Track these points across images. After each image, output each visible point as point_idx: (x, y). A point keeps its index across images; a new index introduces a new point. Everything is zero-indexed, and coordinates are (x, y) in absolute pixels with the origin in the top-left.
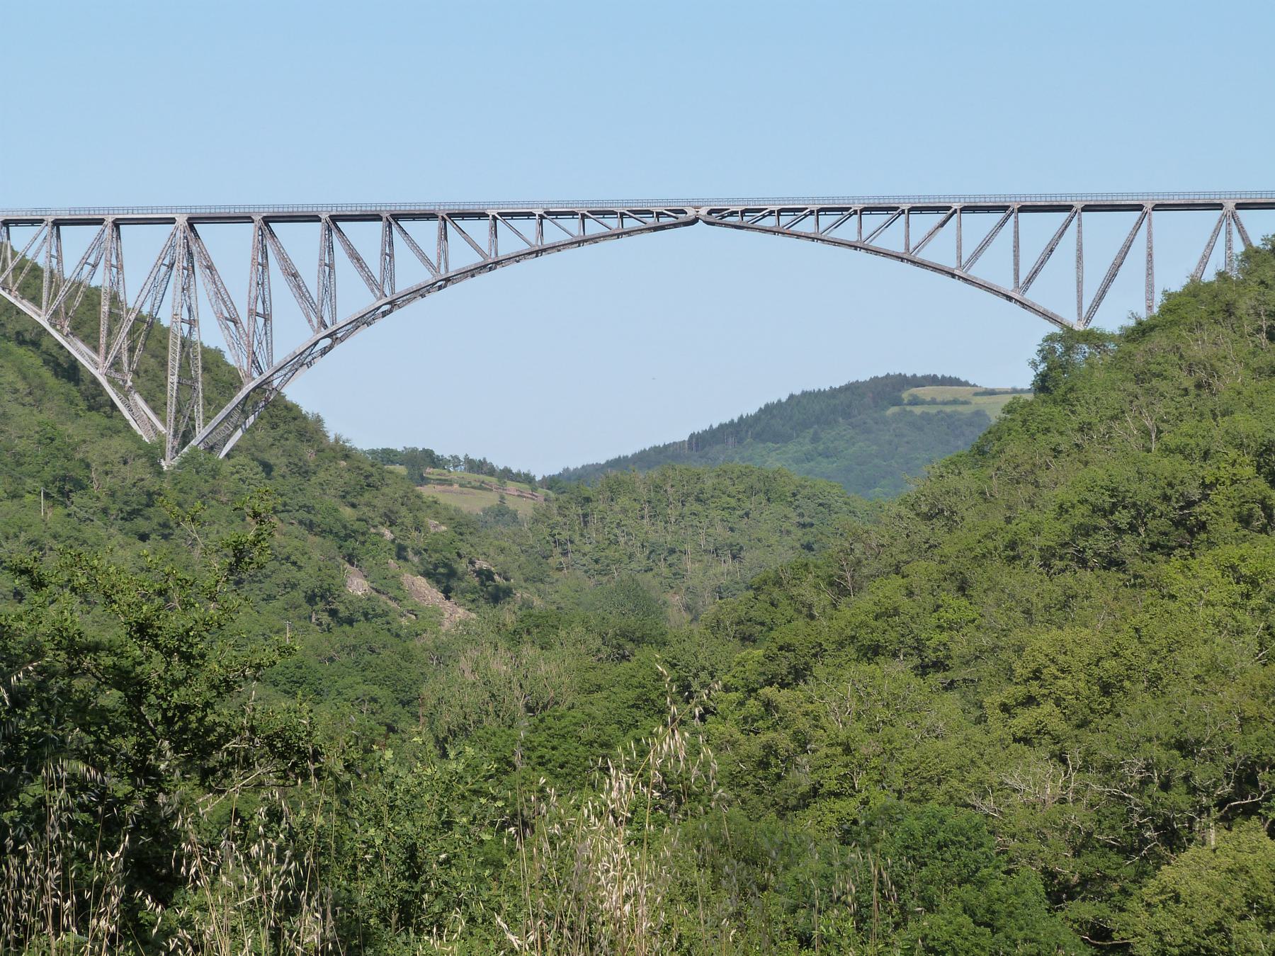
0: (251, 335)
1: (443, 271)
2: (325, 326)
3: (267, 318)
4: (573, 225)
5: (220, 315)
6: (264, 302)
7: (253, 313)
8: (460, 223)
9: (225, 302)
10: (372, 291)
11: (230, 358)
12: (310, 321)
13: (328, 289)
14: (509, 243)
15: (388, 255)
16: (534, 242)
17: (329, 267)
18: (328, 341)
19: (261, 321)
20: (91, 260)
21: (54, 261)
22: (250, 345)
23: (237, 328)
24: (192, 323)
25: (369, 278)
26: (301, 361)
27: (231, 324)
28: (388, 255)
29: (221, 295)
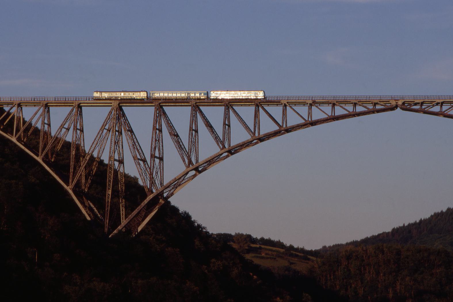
1: (257, 134)
2: (193, 164)
12: (184, 161)
13: (194, 142)
15: (227, 125)
17: (194, 131)
18: (193, 172)
25: (216, 138)
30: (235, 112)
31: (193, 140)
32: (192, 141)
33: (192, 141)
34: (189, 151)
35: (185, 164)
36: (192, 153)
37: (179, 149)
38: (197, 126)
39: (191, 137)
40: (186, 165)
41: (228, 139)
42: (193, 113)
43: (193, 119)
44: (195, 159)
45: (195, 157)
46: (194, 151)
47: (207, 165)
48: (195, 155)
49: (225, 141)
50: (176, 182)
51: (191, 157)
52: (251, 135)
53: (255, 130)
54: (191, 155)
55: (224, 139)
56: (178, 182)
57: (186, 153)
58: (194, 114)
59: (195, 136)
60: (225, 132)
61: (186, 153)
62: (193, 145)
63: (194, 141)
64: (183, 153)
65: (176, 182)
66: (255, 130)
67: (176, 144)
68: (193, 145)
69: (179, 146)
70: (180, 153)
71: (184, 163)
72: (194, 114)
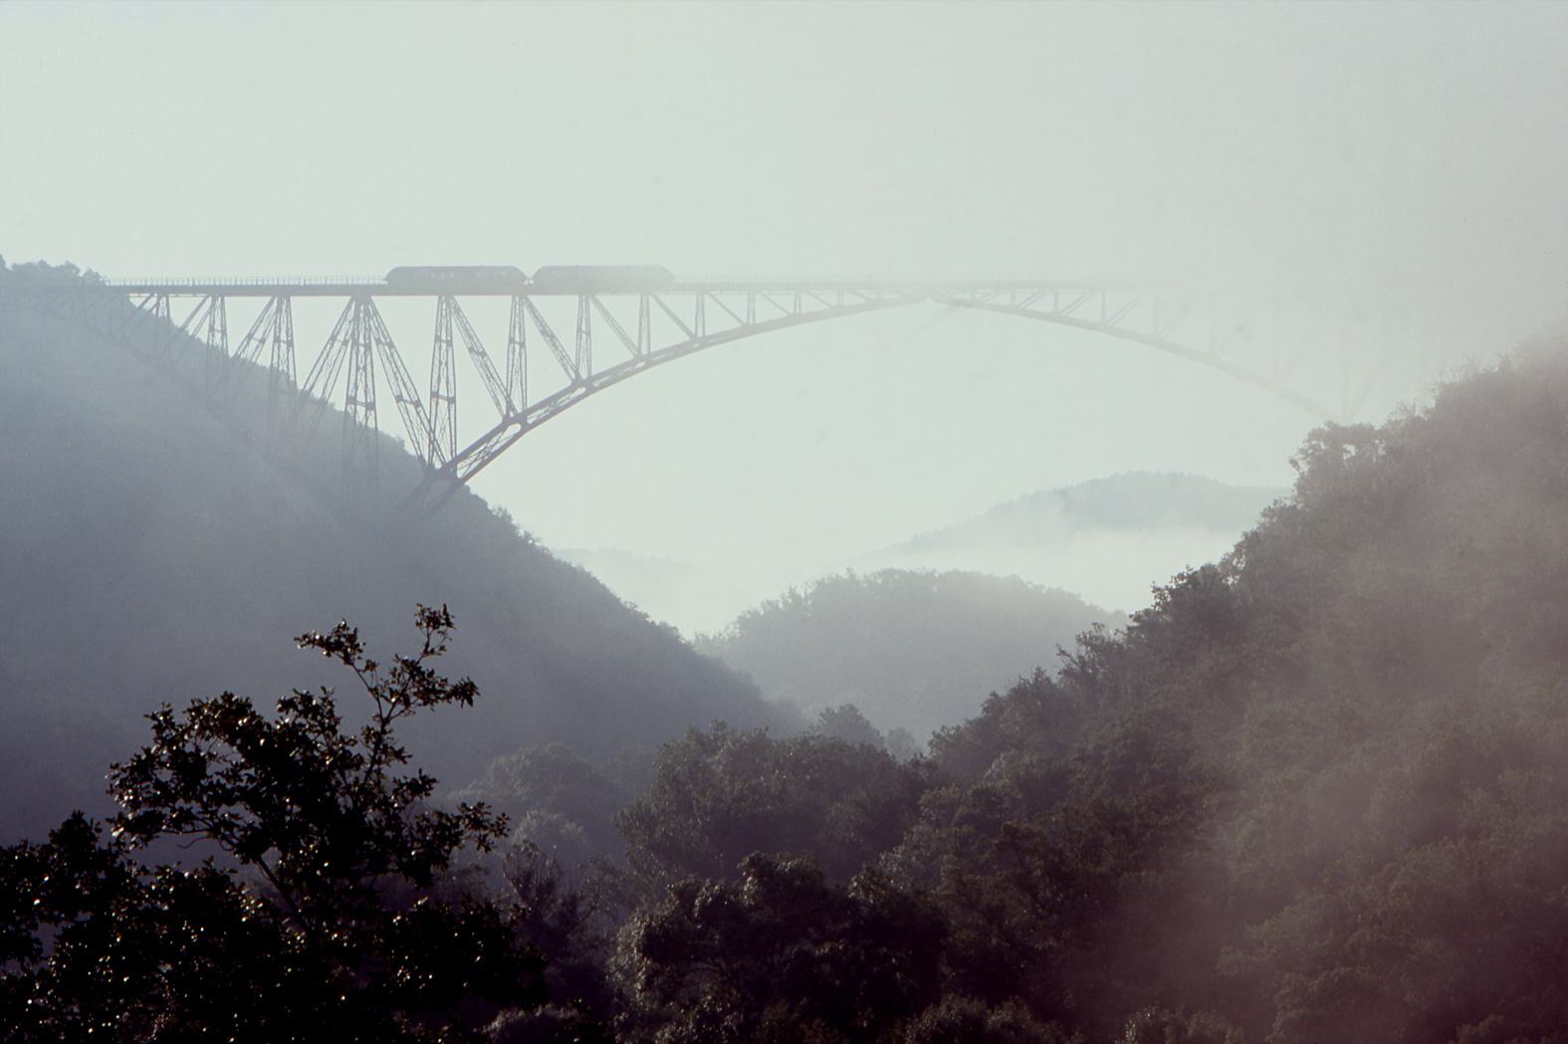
0: (433, 421)
1: (644, 352)
2: (514, 409)
3: (451, 401)
5: (399, 398)
7: (435, 395)
10: (566, 370)
11: (410, 449)
12: (498, 404)
15: (583, 331)
19: (443, 404)
20: (258, 335)
21: (218, 336)
22: (432, 432)
24: (371, 406)
25: (563, 359)
26: (486, 451)
27: (411, 408)
28: (583, 331)
29: (398, 372)
35: (500, 410)
38: (522, 333)
39: (511, 356)
43: (517, 324)
47: (545, 412)
50: (482, 447)
53: (640, 342)
65: (482, 447)
66: (640, 342)
67: (481, 370)
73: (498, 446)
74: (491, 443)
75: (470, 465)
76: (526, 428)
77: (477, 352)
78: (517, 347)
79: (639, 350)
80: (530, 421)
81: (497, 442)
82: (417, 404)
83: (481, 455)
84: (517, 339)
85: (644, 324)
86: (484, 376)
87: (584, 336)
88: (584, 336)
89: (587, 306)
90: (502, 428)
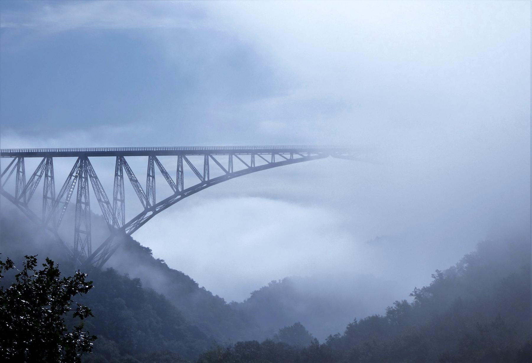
1: (206, 179)
2: (150, 205)
4: (268, 157)
5: (99, 200)
6: (121, 194)
8: (215, 157)
9: (102, 195)
12: (142, 203)
14: (238, 166)
15: (180, 172)
16: (250, 165)
18: (151, 213)
19: (119, 203)
23: (108, 207)
24: (87, 204)
25: (171, 183)
27: (105, 205)
30: (187, 160)
31: (150, 184)
32: (149, 185)
33: (149, 185)
34: (147, 194)
35: (144, 205)
36: (149, 196)
37: (138, 193)
38: (153, 172)
39: (148, 182)
40: (145, 206)
41: (182, 184)
42: (150, 162)
43: (151, 168)
44: (153, 201)
45: (153, 199)
46: (152, 194)
47: (163, 206)
48: (152, 197)
49: (179, 185)
50: (136, 222)
51: (149, 199)
52: (201, 180)
53: (205, 176)
54: (149, 197)
55: (178, 184)
56: (137, 221)
57: (145, 196)
58: (151, 163)
59: (152, 181)
60: (179, 178)
61: (145, 196)
62: (151, 190)
63: (152, 185)
64: (142, 196)
65: (136, 222)
66: (205, 176)
67: (135, 188)
68: (151, 190)
69: (138, 190)
70: (139, 196)
71: (143, 205)
72: (151, 163)
73: (143, 221)
74: (140, 220)
75: (131, 229)
76: (155, 213)
77: (134, 181)
78: (151, 178)
79: (204, 179)
80: (157, 210)
81: (143, 219)
82: (108, 203)
83: (136, 225)
84: (151, 175)
85: (207, 167)
86: (137, 190)
87: (180, 173)
88: (180, 173)
89: (182, 161)
90: (144, 213)
